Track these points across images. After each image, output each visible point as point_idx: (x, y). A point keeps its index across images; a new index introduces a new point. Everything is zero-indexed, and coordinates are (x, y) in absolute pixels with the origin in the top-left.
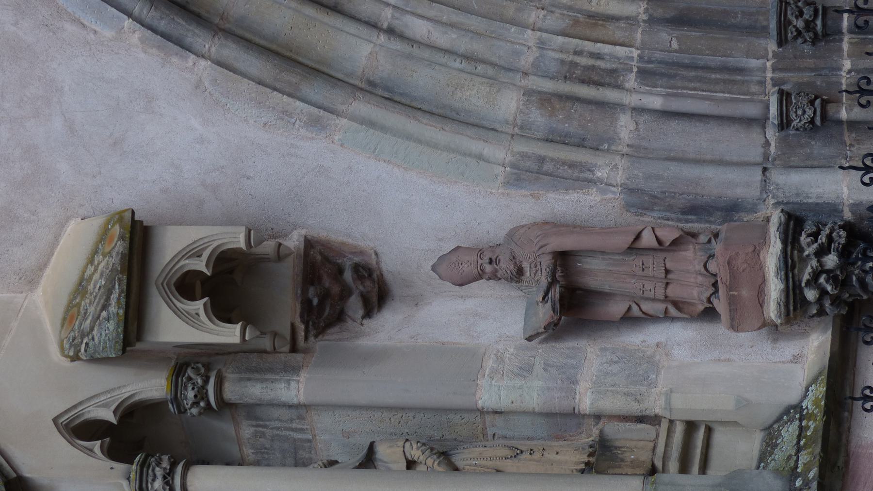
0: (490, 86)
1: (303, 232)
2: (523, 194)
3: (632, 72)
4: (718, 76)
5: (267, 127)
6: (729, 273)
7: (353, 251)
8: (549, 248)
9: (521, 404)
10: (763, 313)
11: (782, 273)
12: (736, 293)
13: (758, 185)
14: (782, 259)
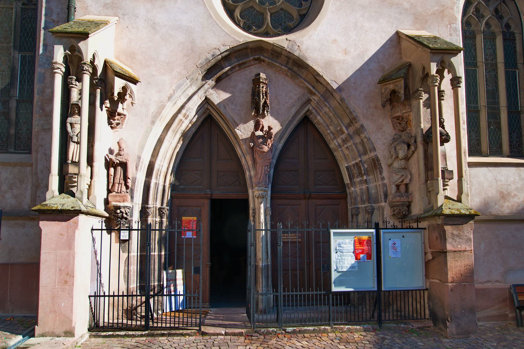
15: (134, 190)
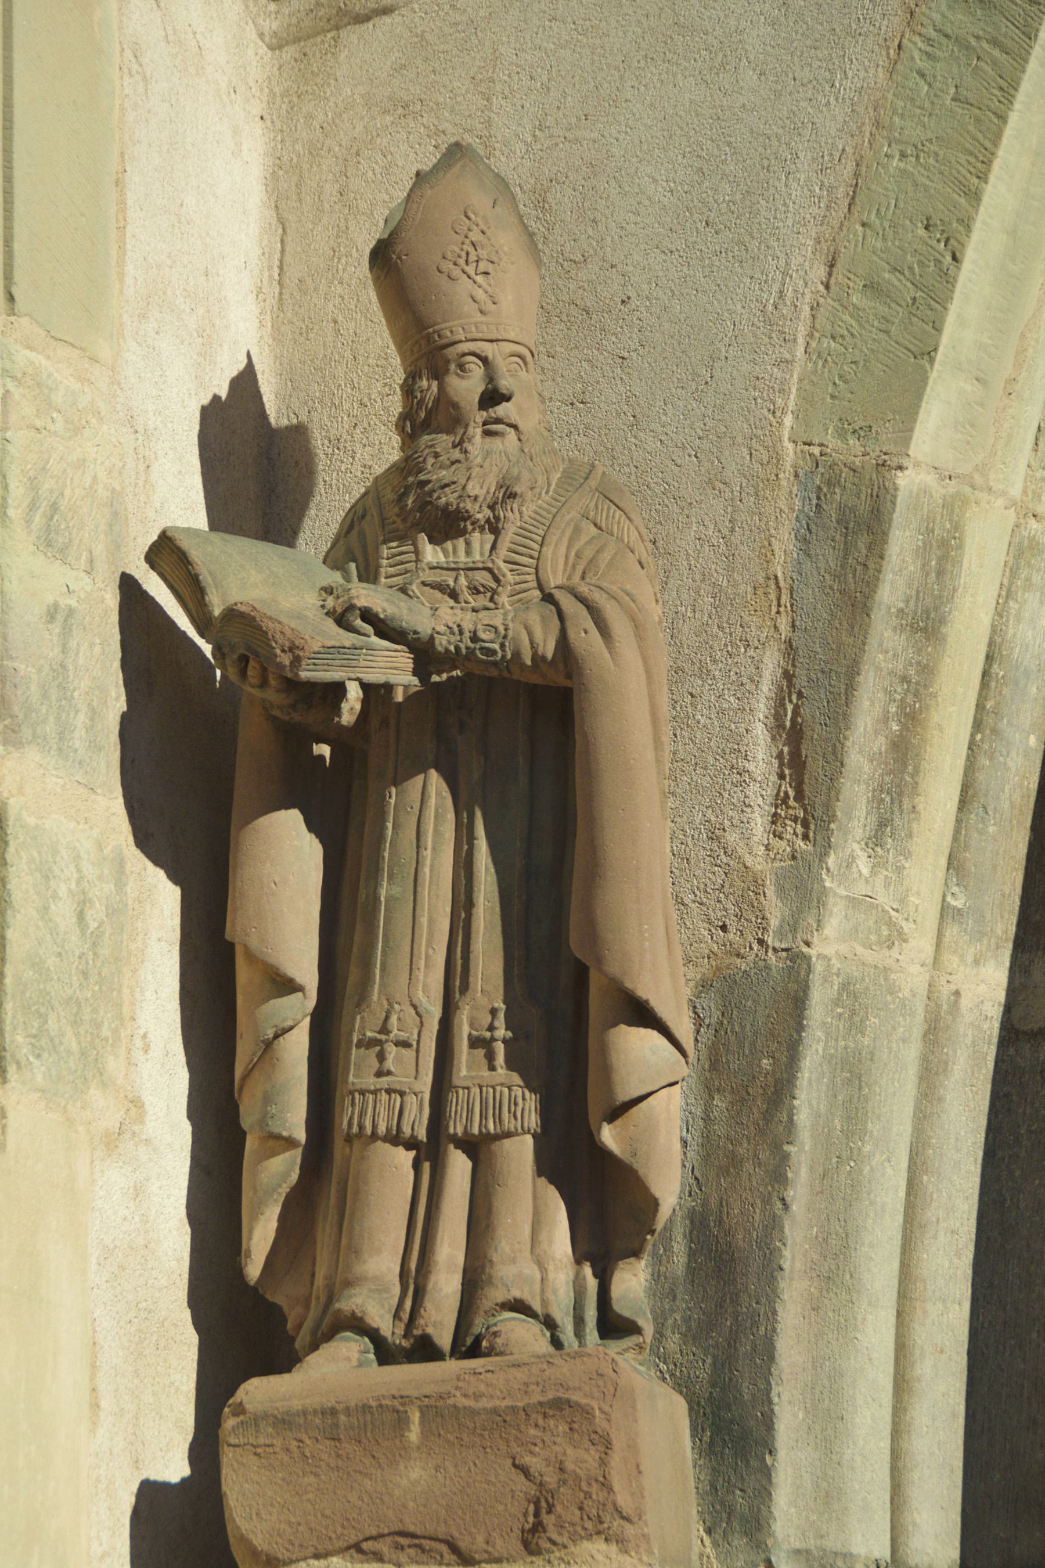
2: (776, 545)
6: (513, 1409)
12: (414, 1435)
15: (771, 1269)
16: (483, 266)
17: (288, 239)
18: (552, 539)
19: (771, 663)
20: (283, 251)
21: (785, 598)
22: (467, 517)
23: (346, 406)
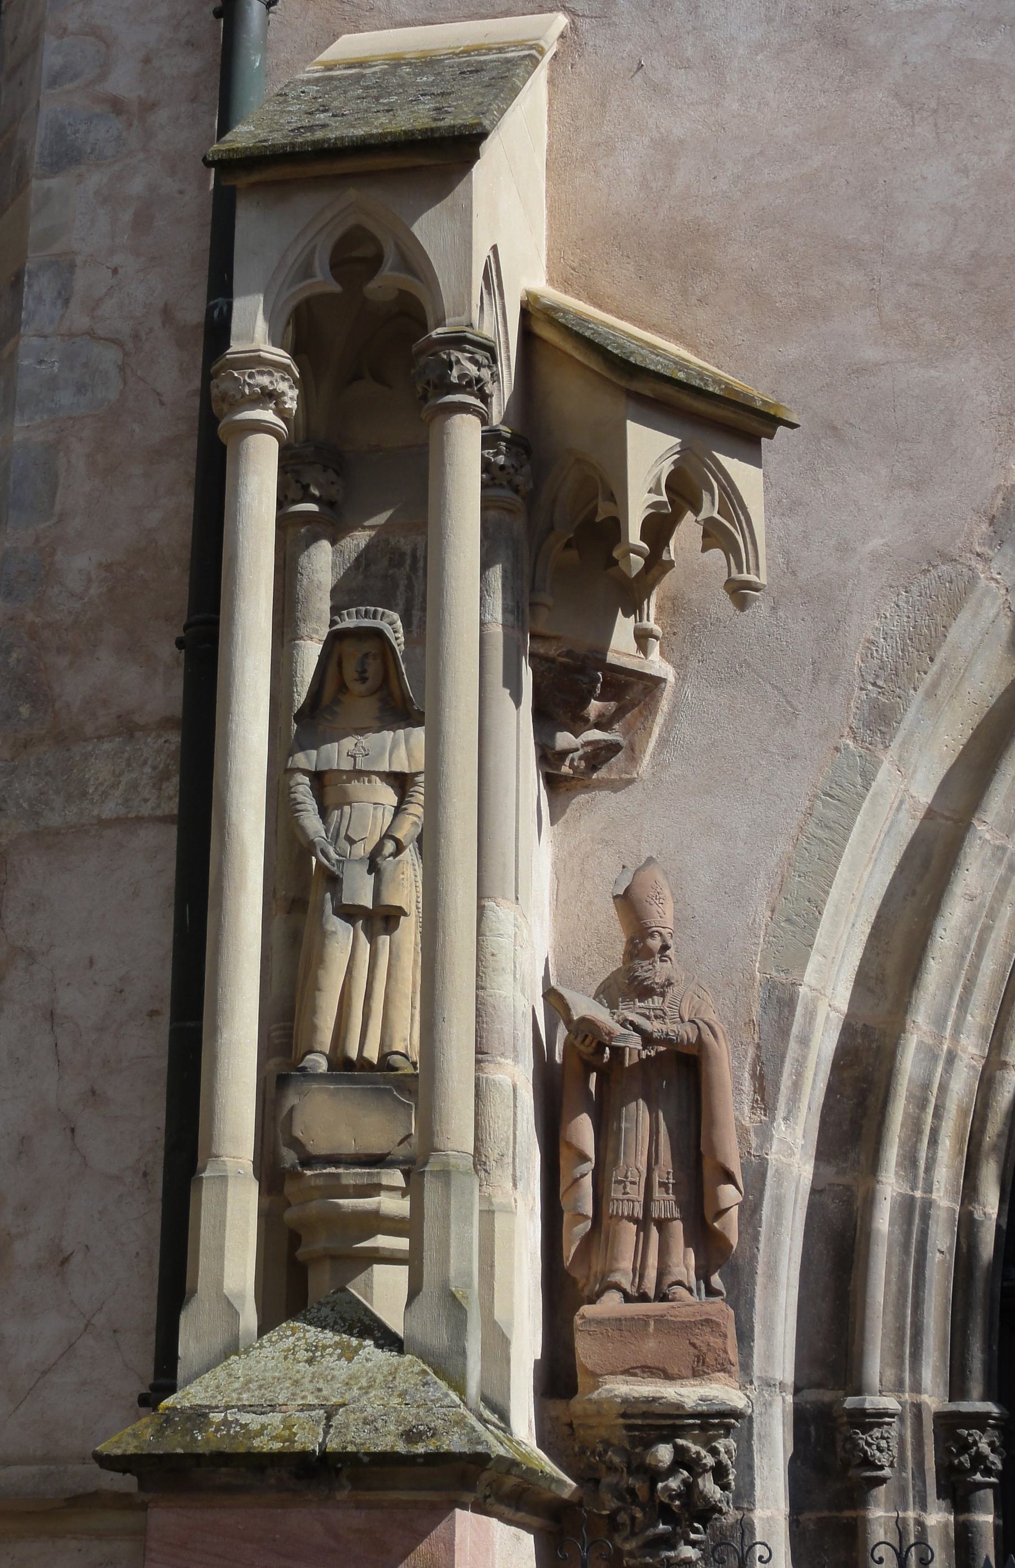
0: (877, 979)
1: (671, 678)
2: (753, 1009)
3: (912, 1190)
4: (909, 1320)
5: (867, 644)
7: (637, 748)
8: (708, 1037)
9: (491, 969)
10: (612, 1374)
11: (705, 1408)
13: (770, 1375)
14: (722, 1408)
15: (753, 1273)
16: (661, 900)
17: (560, 885)
18: (684, 1000)
19: (751, 1052)
20: (558, 889)
21: (757, 1028)
22: (653, 989)
23: (582, 946)
